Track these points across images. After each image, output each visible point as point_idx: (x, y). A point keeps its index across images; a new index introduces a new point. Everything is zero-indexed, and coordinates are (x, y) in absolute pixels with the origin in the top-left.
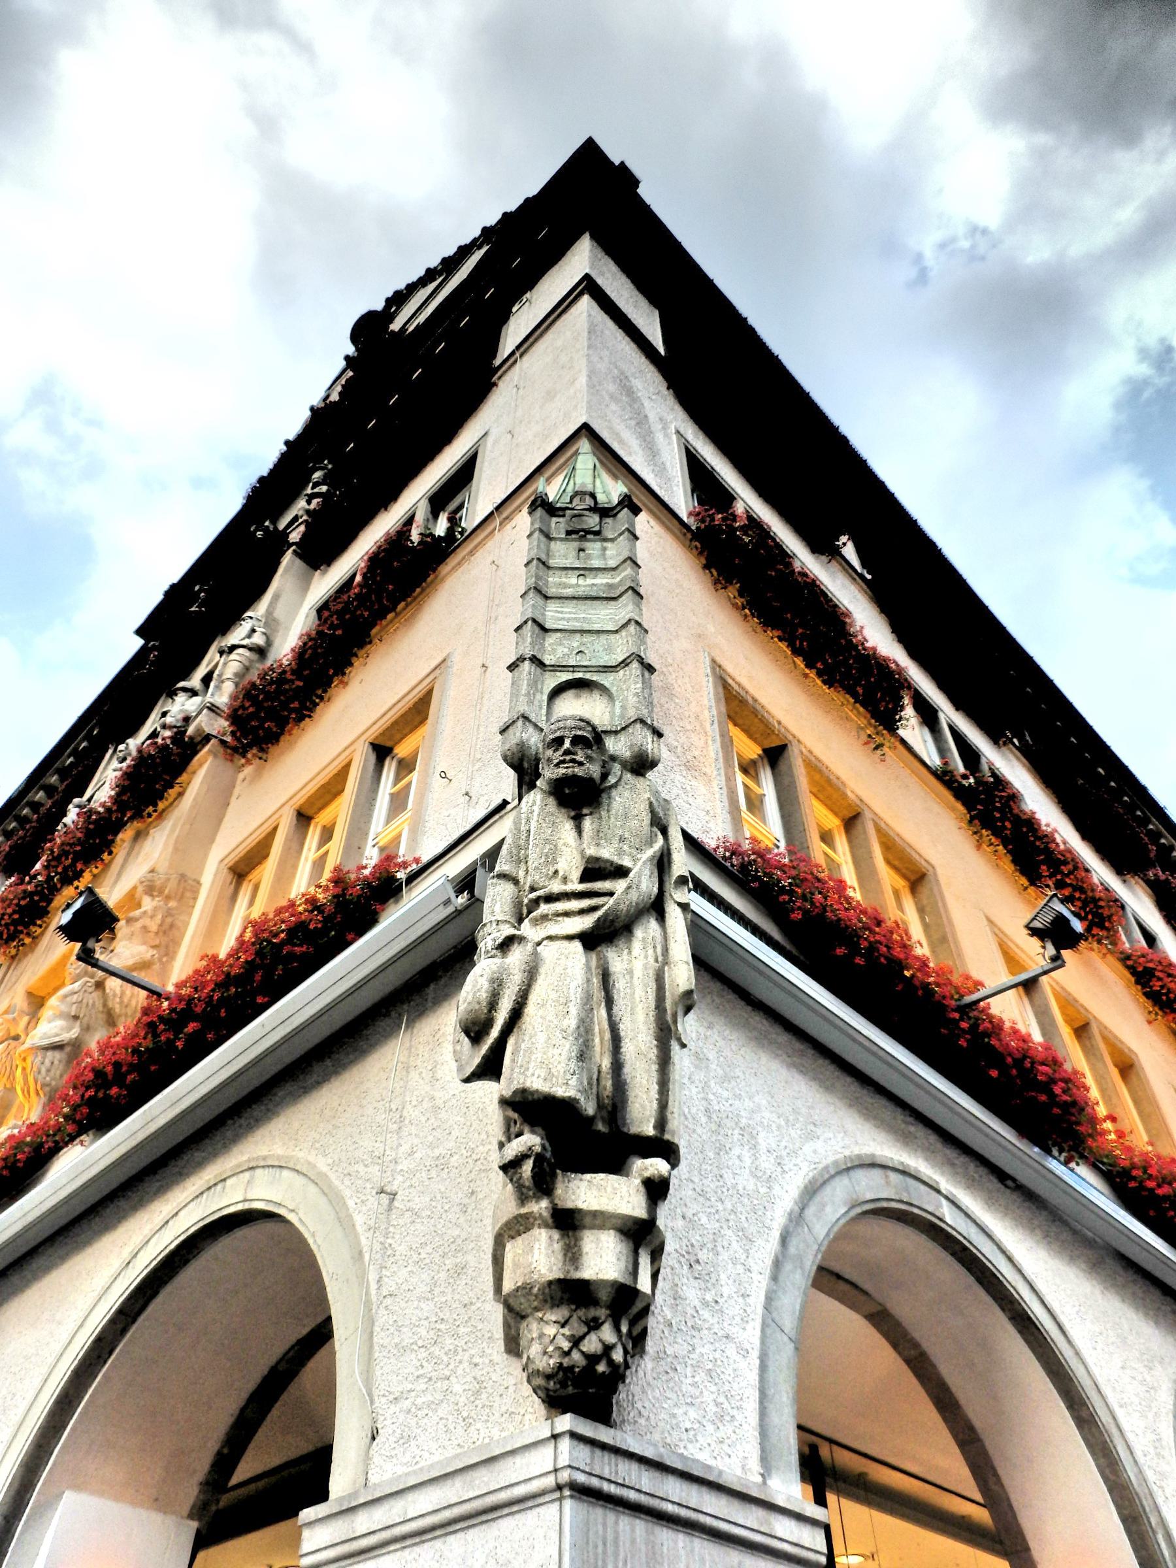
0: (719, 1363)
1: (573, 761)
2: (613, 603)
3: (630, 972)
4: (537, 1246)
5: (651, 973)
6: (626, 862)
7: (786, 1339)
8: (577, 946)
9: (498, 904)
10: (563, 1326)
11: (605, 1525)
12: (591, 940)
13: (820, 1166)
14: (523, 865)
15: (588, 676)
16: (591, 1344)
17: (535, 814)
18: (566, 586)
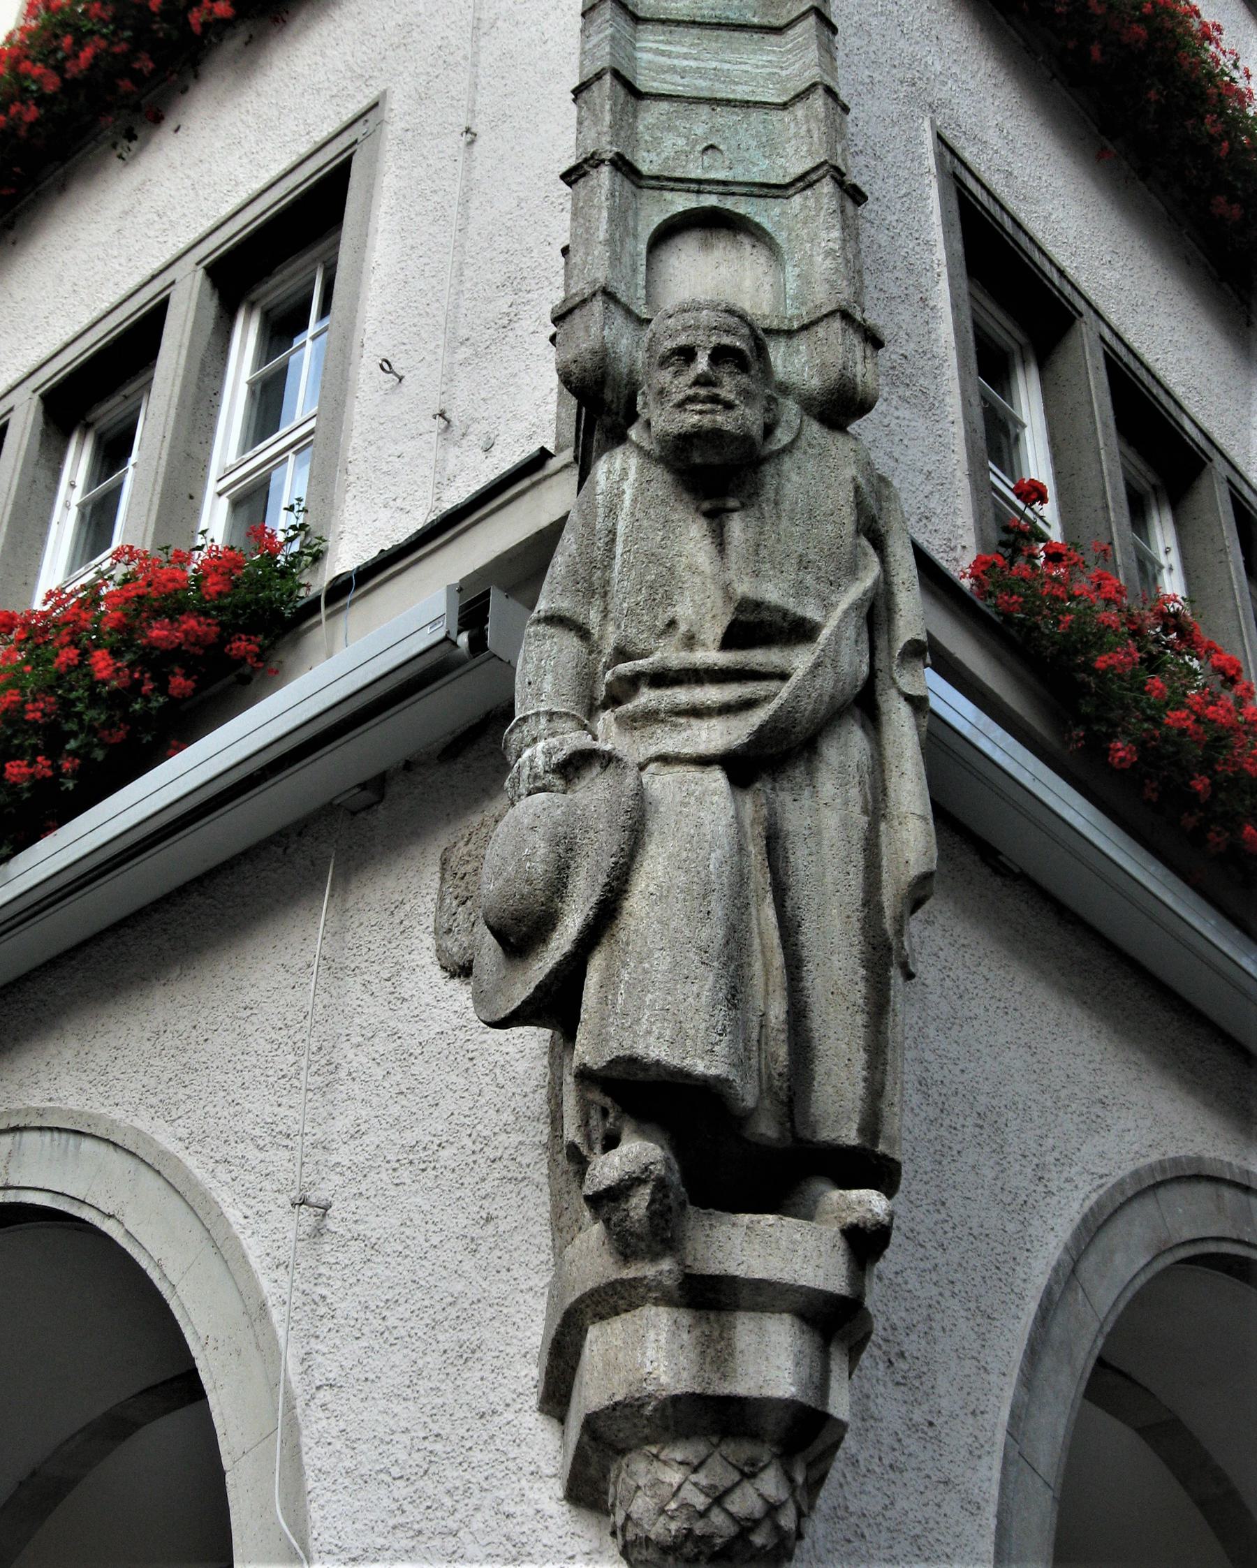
0: (932, 1524)
1: (714, 399)
2: (773, 38)
3: (815, 833)
4: (652, 1335)
5: (857, 836)
6: (811, 612)
7: (1040, 1483)
8: (717, 779)
9: (549, 677)
10: (695, 1470)
12: (742, 768)
13: (1111, 1181)
14: (598, 602)
15: (729, 204)
16: (745, 1502)
17: (627, 498)
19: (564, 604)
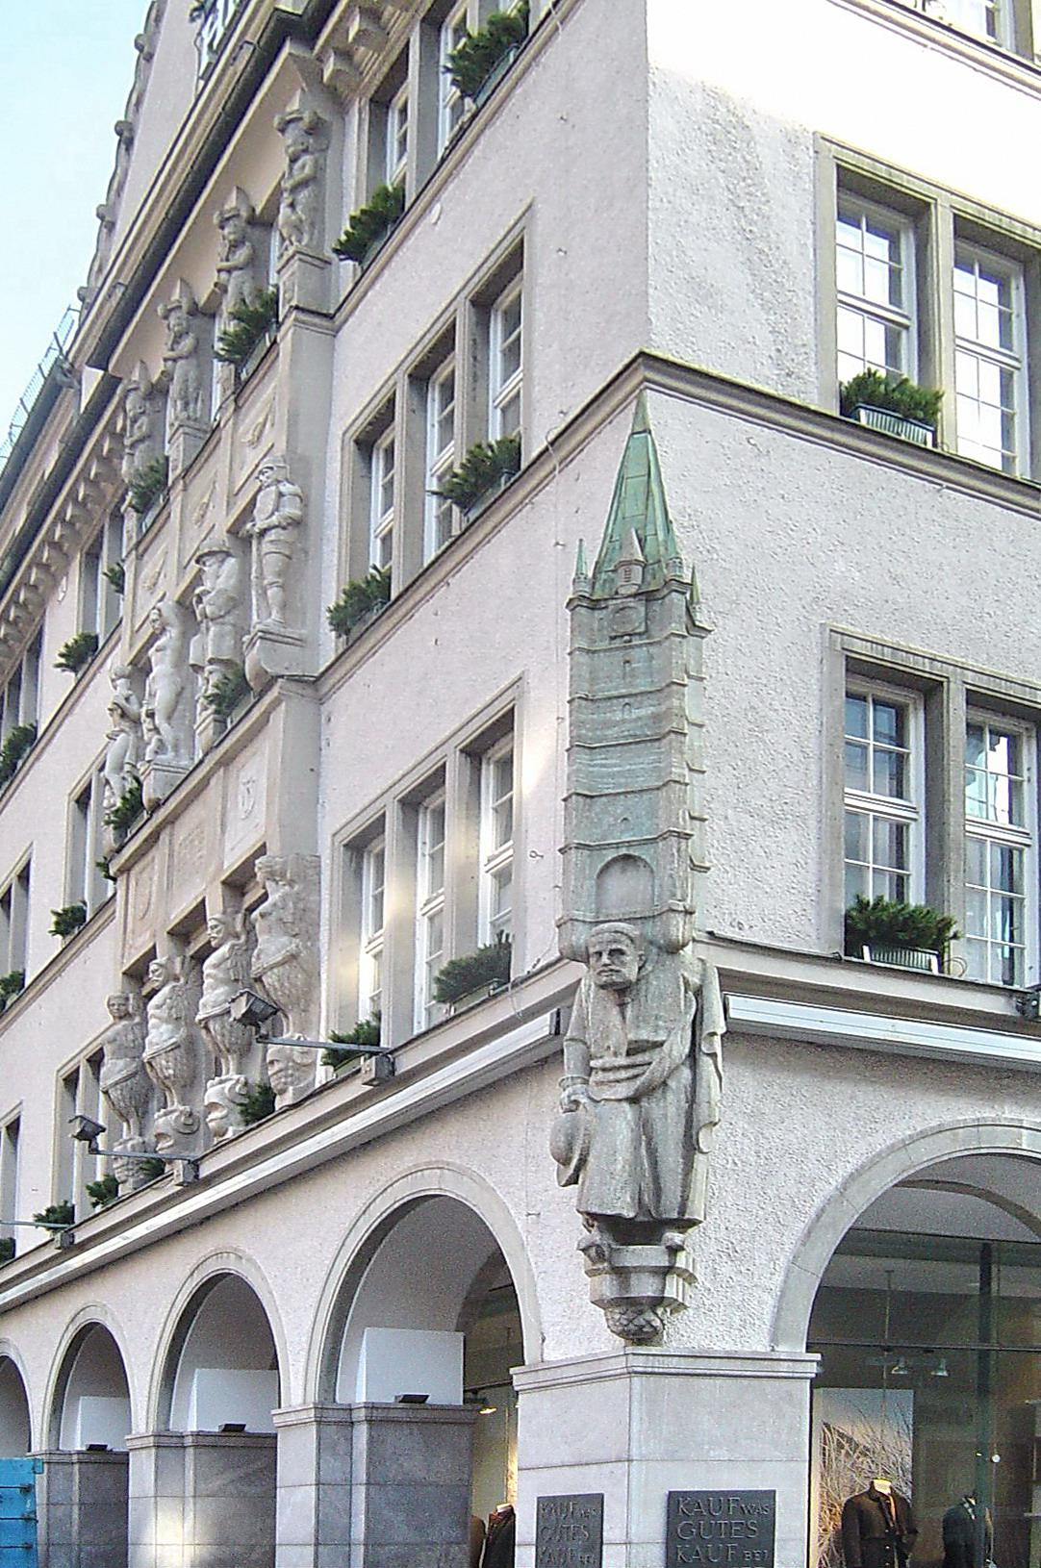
3: (665, 1116)
8: (626, 1106)
12: (633, 1100)
18: (608, 724)
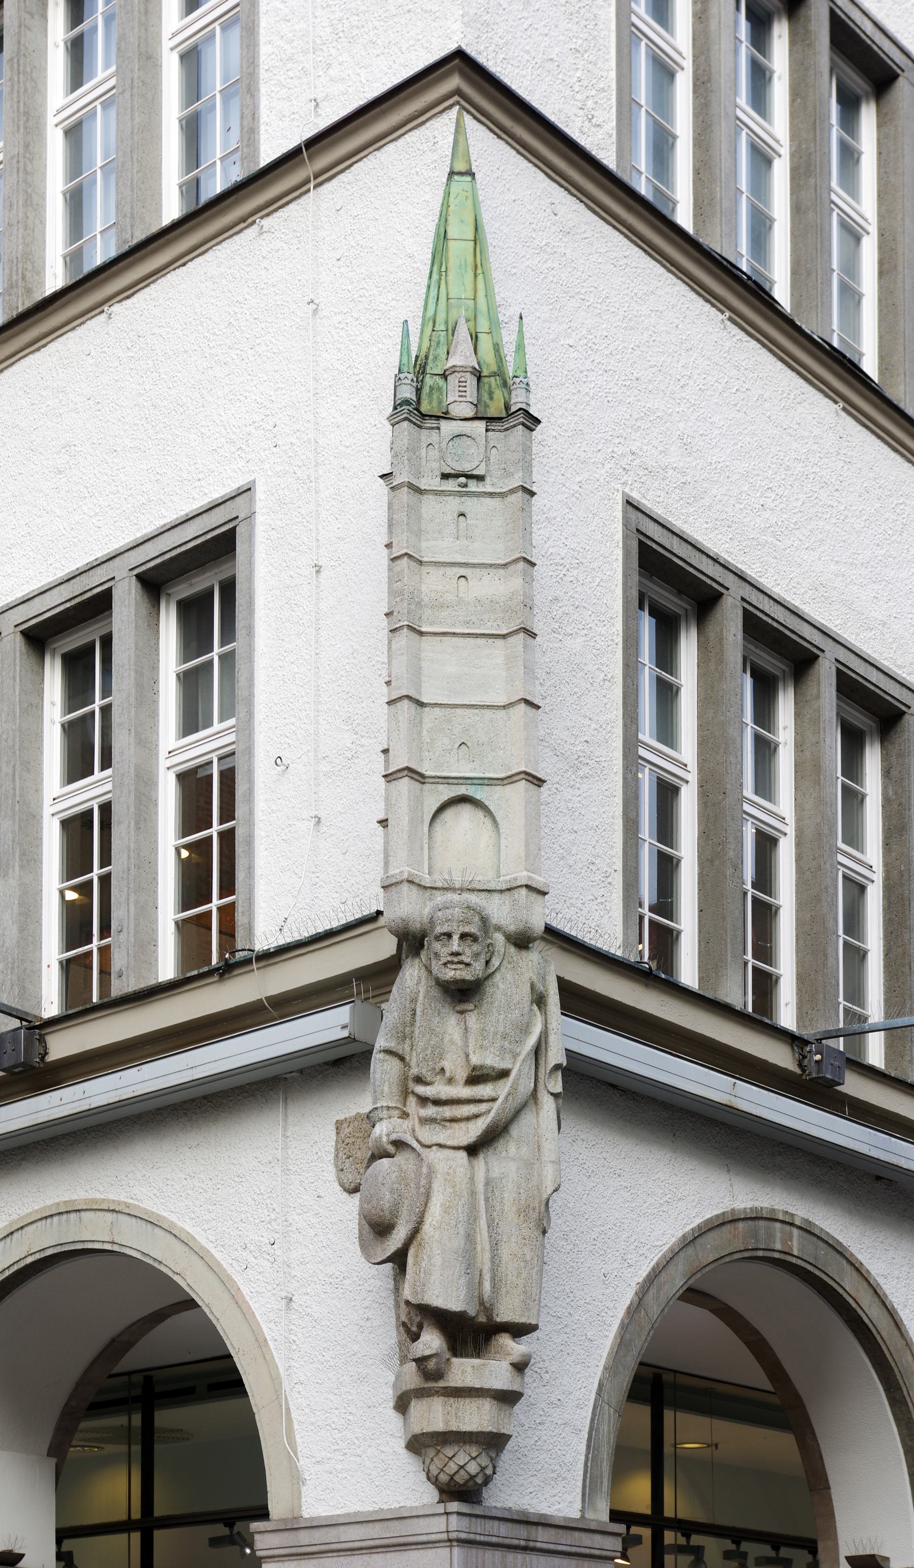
8: (463, 1154)
11: (477, 1558)
12: (472, 1150)
14: (408, 1041)
19: (392, 1045)
